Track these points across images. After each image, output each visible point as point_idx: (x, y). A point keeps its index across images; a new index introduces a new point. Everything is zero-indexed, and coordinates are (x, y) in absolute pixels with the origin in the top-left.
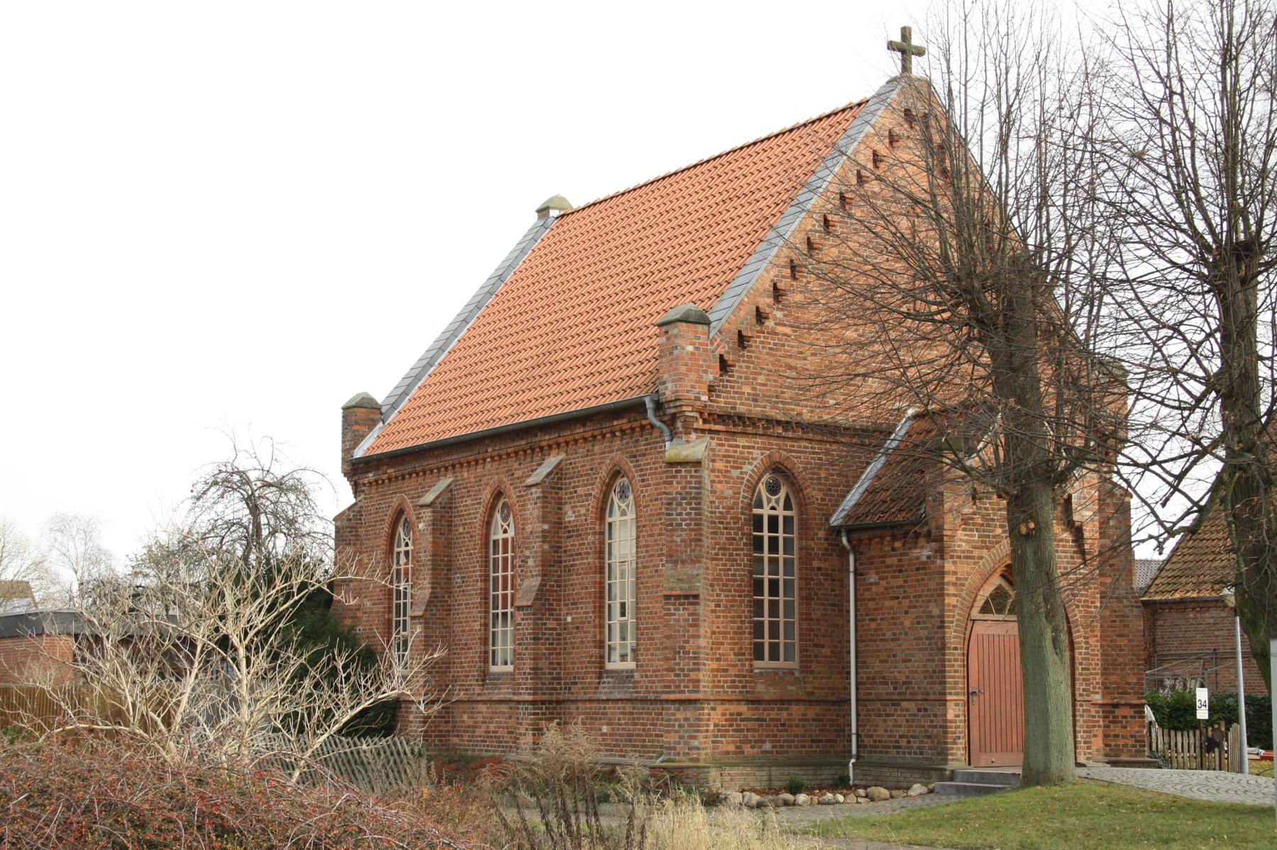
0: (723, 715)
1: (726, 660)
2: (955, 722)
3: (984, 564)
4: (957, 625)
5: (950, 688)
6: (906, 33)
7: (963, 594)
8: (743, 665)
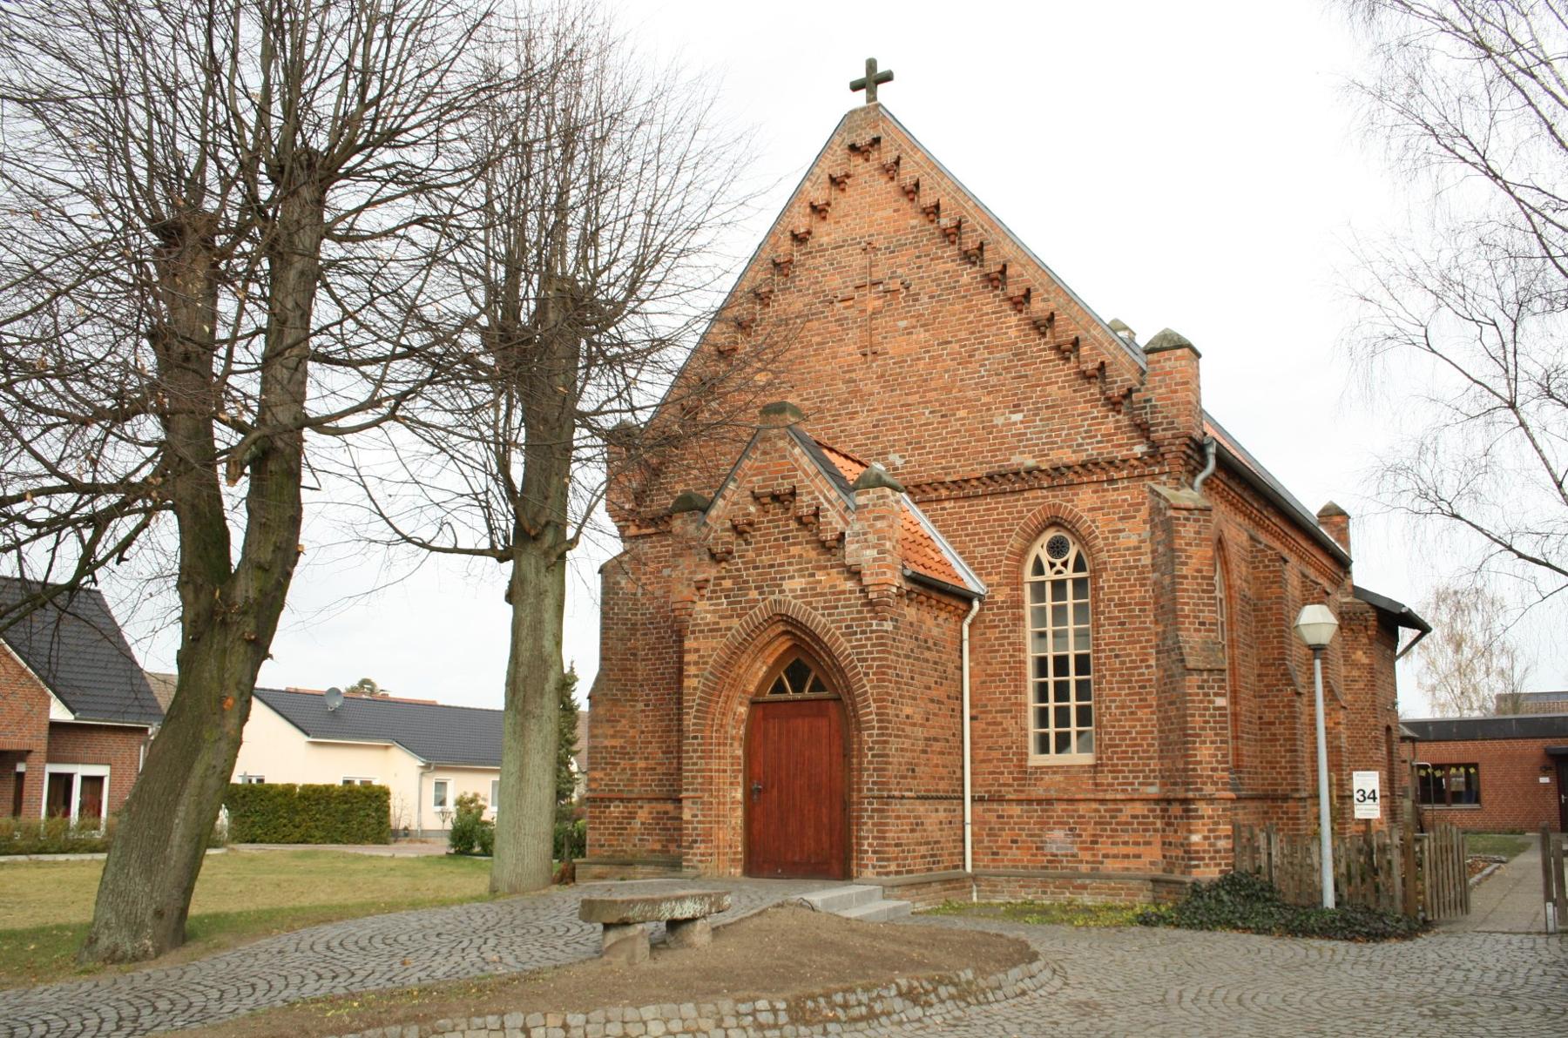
0: (651, 813)
1: (653, 759)
2: (692, 823)
3: (733, 636)
4: (697, 711)
5: (687, 784)
6: (887, 77)
7: (706, 673)
8: (671, 763)
